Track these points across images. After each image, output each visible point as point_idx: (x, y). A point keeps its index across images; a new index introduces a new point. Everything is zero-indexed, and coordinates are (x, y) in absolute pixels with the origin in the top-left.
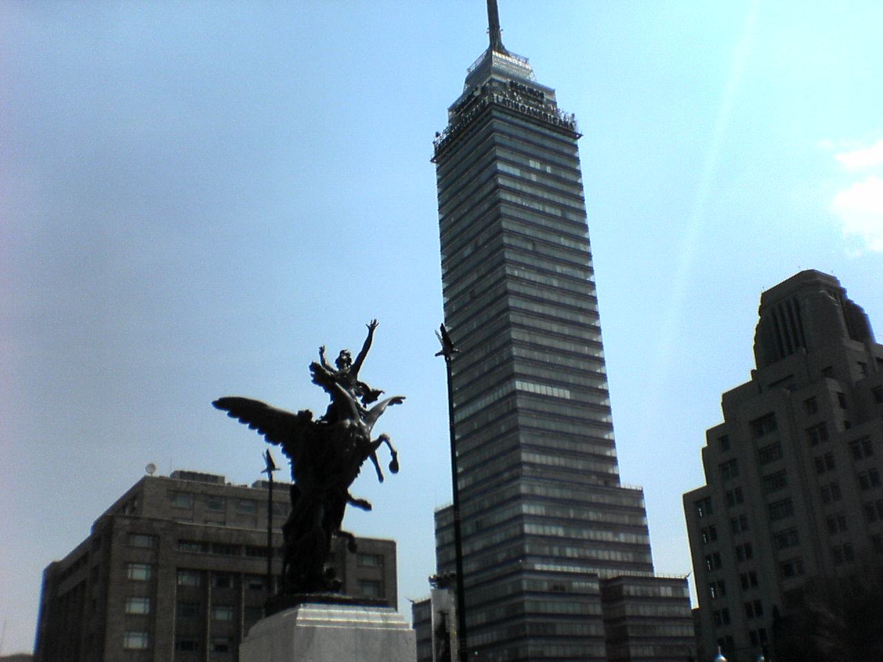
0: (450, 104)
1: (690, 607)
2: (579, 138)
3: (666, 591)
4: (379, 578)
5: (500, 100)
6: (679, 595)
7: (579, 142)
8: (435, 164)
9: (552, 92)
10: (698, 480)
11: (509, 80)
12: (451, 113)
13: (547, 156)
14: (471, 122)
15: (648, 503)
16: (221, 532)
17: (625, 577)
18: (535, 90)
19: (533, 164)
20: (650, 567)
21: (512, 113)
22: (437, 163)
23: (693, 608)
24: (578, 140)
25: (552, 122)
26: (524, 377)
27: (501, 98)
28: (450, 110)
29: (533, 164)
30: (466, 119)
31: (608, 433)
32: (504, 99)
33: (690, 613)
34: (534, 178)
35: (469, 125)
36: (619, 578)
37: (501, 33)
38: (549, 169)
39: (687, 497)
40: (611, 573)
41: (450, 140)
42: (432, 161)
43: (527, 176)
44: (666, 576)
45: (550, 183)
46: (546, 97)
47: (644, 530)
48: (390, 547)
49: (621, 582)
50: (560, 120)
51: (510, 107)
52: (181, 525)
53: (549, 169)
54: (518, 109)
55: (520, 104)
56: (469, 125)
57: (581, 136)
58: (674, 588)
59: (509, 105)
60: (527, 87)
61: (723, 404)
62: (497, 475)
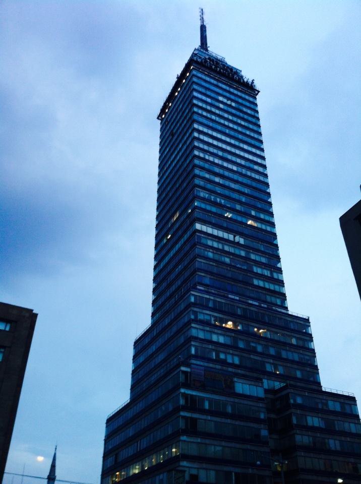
2: (257, 94)
13: (233, 97)
15: (314, 330)
19: (221, 98)
26: (204, 222)
29: (221, 98)
32: (202, 61)
34: (221, 106)
38: (233, 104)
42: (158, 118)
43: (217, 104)
44: (335, 392)
53: (233, 104)
57: (259, 92)
58: (342, 404)
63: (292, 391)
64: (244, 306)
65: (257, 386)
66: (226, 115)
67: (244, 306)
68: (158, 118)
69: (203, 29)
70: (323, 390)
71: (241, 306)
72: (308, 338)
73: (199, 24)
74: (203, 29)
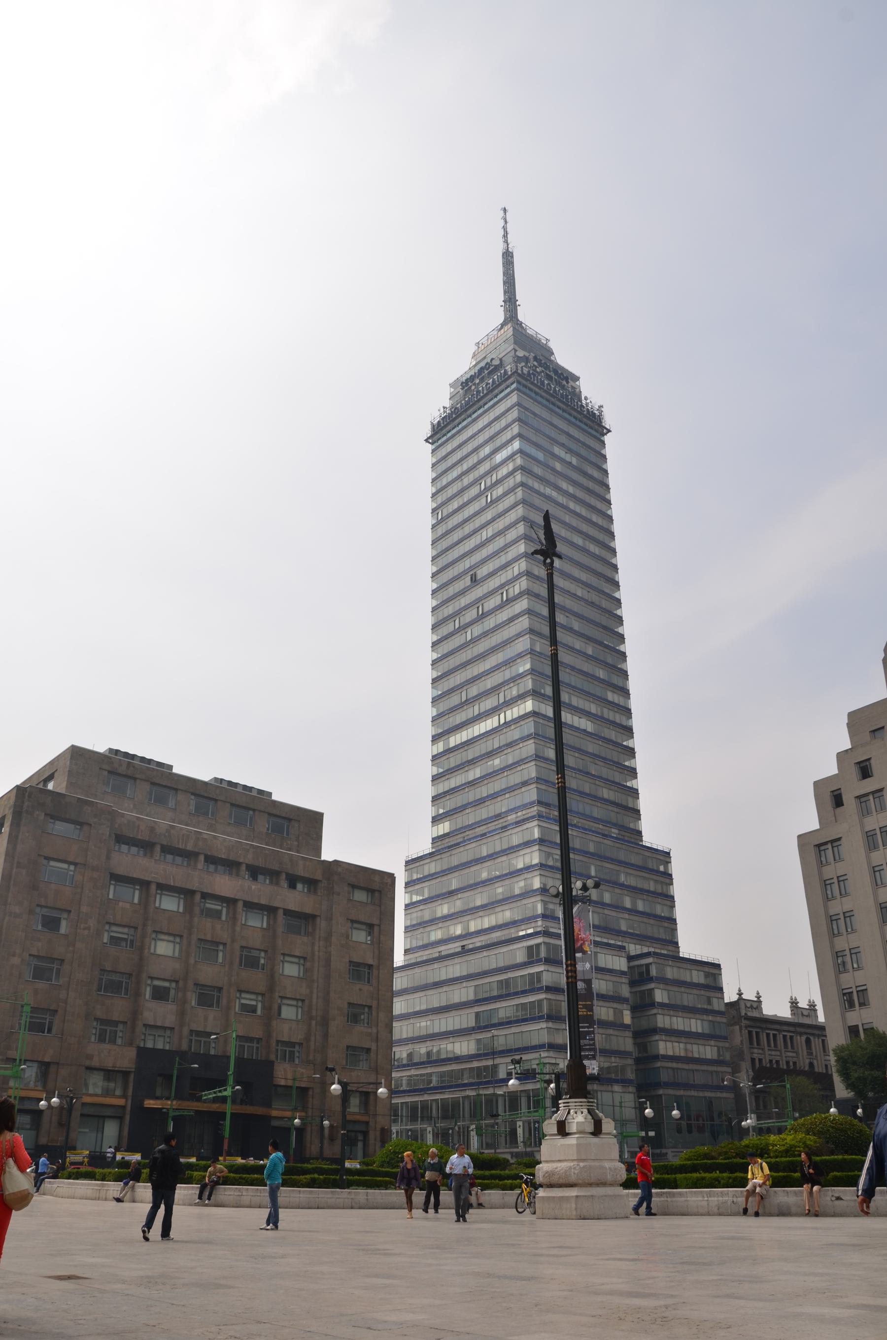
0: (452, 380)
1: (723, 999)
2: (606, 434)
3: (697, 977)
4: (376, 921)
5: (525, 372)
6: (712, 984)
7: (607, 439)
8: (430, 445)
9: (577, 379)
10: (811, 822)
11: (533, 355)
12: (452, 390)
14: (487, 394)
15: (676, 868)
16: (172, 831)
17: (655, 953)
18: (560, 372)
19: (557, 450)
20: (676, 944)
21: (537, 390)
22: (432, 444)
23: (727, 1000)
24: (605, 436)
25: (579, 409)
27: (526, 370)
28: (451, 386)
29: (557, 450)
30: (478, 392)
31: (631, 780)
33: (723, 1009)
34: (558, 466)
35: (482, 398)
36: (648, 955)
37: (518, 307)
39: (799, 837)
40: (634, 949)
41: (454, 416)
42: (427, 441)
45: (575, 476)
46: (571, 383)
47: (670, 899)
48: (389, 881)
49: (650, 960)
50: (588, 409)
51: (536, 382)
52: (123, 815)
53: (574, 461)
54: (544, 386)
55: (546, 382)
56: (482, 398)
57: (609, 431)
58: (707, 975)
59: (534, 380)
60: (551, 366)
61: (849, 725)
62: (498, 816)
63: (656, 960)
64: (598, 839)
65: (619, 956)
66: (564, 485)
67: (598, 839)
68: (427, 441)
69: (508, 258)
70: (681, 955)
71: (594, 838)
72: (668, 881)
73: (500, 248)
74: (508, 258)
